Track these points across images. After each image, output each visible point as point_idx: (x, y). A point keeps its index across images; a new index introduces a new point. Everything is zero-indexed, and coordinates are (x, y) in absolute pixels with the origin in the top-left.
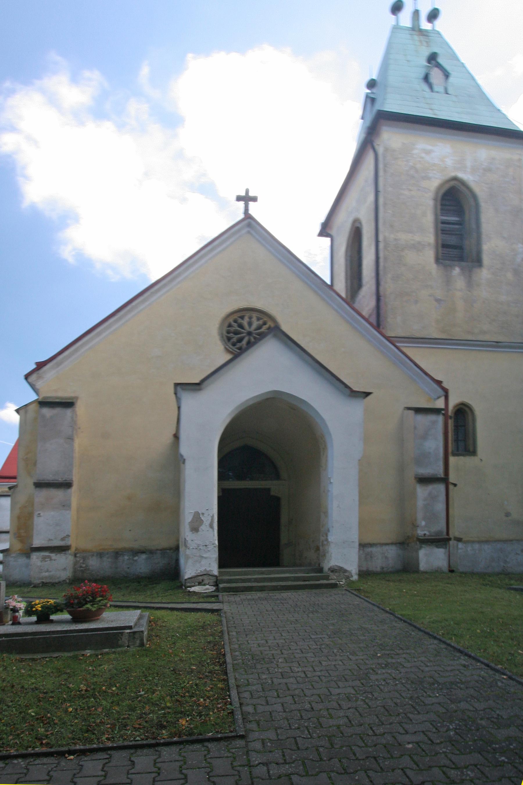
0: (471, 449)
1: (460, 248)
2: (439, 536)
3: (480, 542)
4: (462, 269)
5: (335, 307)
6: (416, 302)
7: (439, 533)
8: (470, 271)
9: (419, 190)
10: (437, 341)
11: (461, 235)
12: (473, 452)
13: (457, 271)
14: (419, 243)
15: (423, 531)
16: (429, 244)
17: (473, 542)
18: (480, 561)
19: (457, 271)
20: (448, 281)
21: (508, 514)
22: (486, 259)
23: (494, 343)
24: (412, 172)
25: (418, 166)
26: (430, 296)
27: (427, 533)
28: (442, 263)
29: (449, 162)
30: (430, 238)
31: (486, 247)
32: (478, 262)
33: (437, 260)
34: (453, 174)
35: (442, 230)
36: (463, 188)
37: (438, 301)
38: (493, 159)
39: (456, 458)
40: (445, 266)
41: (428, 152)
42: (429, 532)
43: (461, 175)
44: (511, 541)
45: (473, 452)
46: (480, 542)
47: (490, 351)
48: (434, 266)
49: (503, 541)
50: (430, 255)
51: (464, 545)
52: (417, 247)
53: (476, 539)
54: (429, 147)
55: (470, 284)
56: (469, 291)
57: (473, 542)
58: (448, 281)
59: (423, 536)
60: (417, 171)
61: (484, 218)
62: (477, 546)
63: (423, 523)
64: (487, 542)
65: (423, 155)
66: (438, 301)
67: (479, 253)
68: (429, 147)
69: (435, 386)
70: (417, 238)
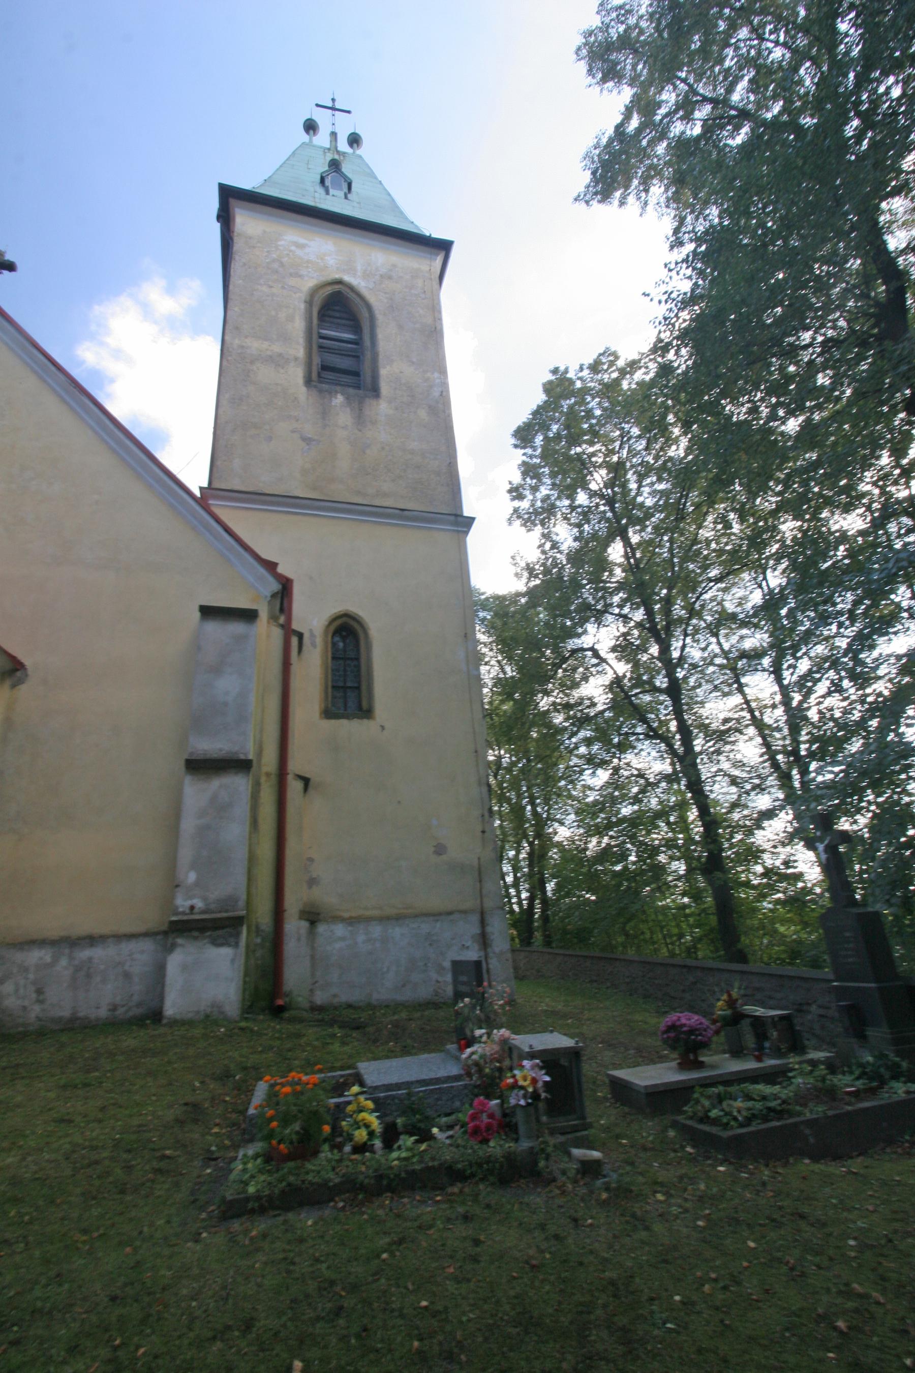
0: (365, 705)
1: (357, 374)
2: (227, 911)
3: (384, 919)
4: (348, 398)
5: (93, 424)
6: (269, 439)
7: (229, 901)
8: (361, 402)
9: (283, 288)
10: (298, 501)
11: (358, 357)
12: (365, 712)
13: (339, 399)
14: (280, 355)
15: (191, 898)
16: (296, 359)
17: (369, 920)
18: (385, 970)
19: (339, 399)
20: (325, 413)
21: (440, 850)
22: (385, 389)
23: (397, 511)
24: (275, 266)
25: (285, 260)
26: (293, 432)
27: (199, 904)
28: (315, 387)
29: (331, 261)
30: (299, 351)
31: (384, 372)
32: (375, 391)
33: (308, 382)
34: (337, 276)
35: (321, 347)
36: (352, 295)
37: (307, 440)
38: (394, 266)
39: (333, 721)
40: (321, 391)
41: (302, 246)
42: (204, 899)
43: (347, 278)
44: (450, 913)
45: (365, 712)
46: (384, 919)
47: (389, 524)
48: (304, 389)
49: (434, 915)
50: (297, 374)
51: (350, 928)
52: (278, 361)
53: (376, 913)
54: (302, 241)
55: (360, 419)
56: (360, 431)
57: (369, 920)
58: (325, 413)
59: (188, 911)
60: (282, 265)
61: (381, 335)
62: (376, 930)
63: (192, 877)
64: (398, 918)
65: (293, 248)
66: (307, 440)
67: (375, 378)
68: (302, 241)
69: (262, 571)
70: (277, 348)
